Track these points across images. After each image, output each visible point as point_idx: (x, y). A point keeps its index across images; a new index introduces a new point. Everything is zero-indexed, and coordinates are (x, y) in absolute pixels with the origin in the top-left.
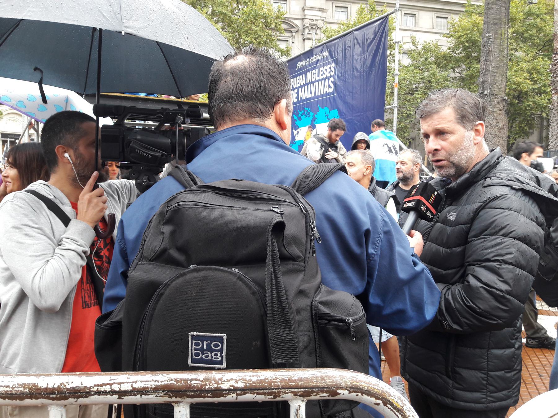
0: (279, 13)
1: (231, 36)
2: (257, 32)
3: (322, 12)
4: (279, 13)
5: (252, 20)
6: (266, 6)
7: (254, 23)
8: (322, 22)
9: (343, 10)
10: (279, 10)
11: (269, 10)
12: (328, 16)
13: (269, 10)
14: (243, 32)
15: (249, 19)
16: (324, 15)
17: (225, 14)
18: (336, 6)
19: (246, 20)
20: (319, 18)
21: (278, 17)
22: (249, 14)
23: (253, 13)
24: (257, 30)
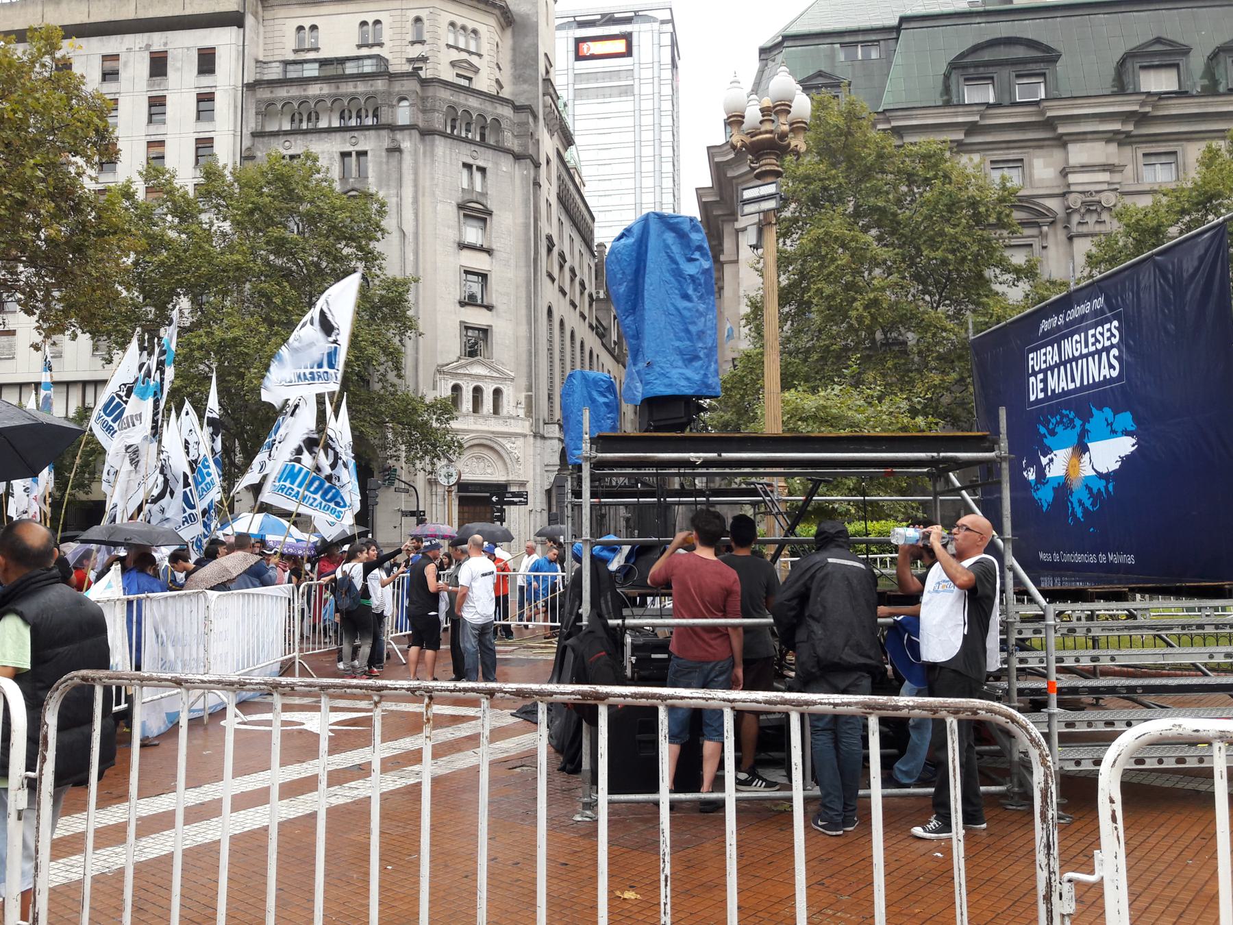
3: (1111, 171)
8: (1112, 195)
9: (1164, 159)
12: (1126, 179)
16: (1117, 178)
18: (1145, 155)
20: (1105, 187)
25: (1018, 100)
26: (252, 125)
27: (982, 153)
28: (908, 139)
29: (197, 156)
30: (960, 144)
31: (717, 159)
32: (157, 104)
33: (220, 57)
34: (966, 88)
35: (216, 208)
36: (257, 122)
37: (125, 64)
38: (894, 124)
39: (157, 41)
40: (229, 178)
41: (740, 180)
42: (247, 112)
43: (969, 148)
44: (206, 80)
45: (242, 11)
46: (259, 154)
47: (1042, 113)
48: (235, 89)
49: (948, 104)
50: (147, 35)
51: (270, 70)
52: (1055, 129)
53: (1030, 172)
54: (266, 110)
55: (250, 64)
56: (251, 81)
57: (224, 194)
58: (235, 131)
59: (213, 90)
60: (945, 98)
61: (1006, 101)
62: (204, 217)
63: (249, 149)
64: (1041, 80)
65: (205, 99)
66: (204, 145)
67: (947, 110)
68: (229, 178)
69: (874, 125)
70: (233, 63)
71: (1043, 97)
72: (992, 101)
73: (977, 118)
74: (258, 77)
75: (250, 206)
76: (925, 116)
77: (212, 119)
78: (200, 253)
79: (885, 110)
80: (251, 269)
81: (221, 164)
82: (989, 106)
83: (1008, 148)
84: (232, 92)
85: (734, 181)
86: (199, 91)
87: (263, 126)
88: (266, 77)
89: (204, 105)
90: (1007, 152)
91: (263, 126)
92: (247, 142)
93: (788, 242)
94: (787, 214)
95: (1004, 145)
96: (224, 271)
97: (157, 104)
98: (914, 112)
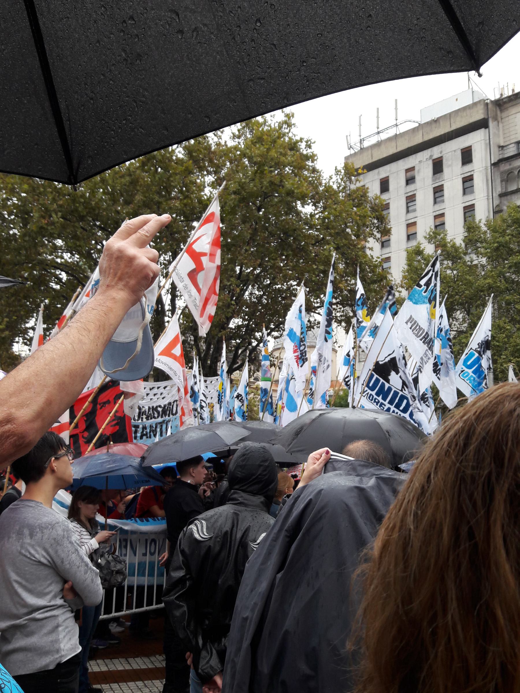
26: (499, 190)
29: (465, 218)
32: (438, 191)
33: (475, 151)
35: (476, 249)
36: (502, 187)
37: (419, 172)
39: (436, 152)
40: (484, 228)
42: (495, 182)
44: (468, 168)
45: (486, 117)
46: (505, 208)
48: (486, 169)
50: (430, 150)
51: (508, 151)
54: (507, 177)
55: (495, 149)
56: (496, 161)
57: (480, 240)
58: (488, 196)
59: (472, 173)
62: (467, 258)
63: (498, 206)
65: (468, 180)
66: (469, 210)
68: (484, 228)
70: (484, 152)
74: (501, 157)
75: (496, 245)
77: (472, 192)
78: (464, 282)
80: (499, 287)
81: (477, 221)
84: (484, 172)
86: (463, 176)
87: (506, 188)
88: (506, 156)
89: (467, 184)
91: (506, 188)
92: (497, 202)
96: (482, 291)
97: (438, 191)
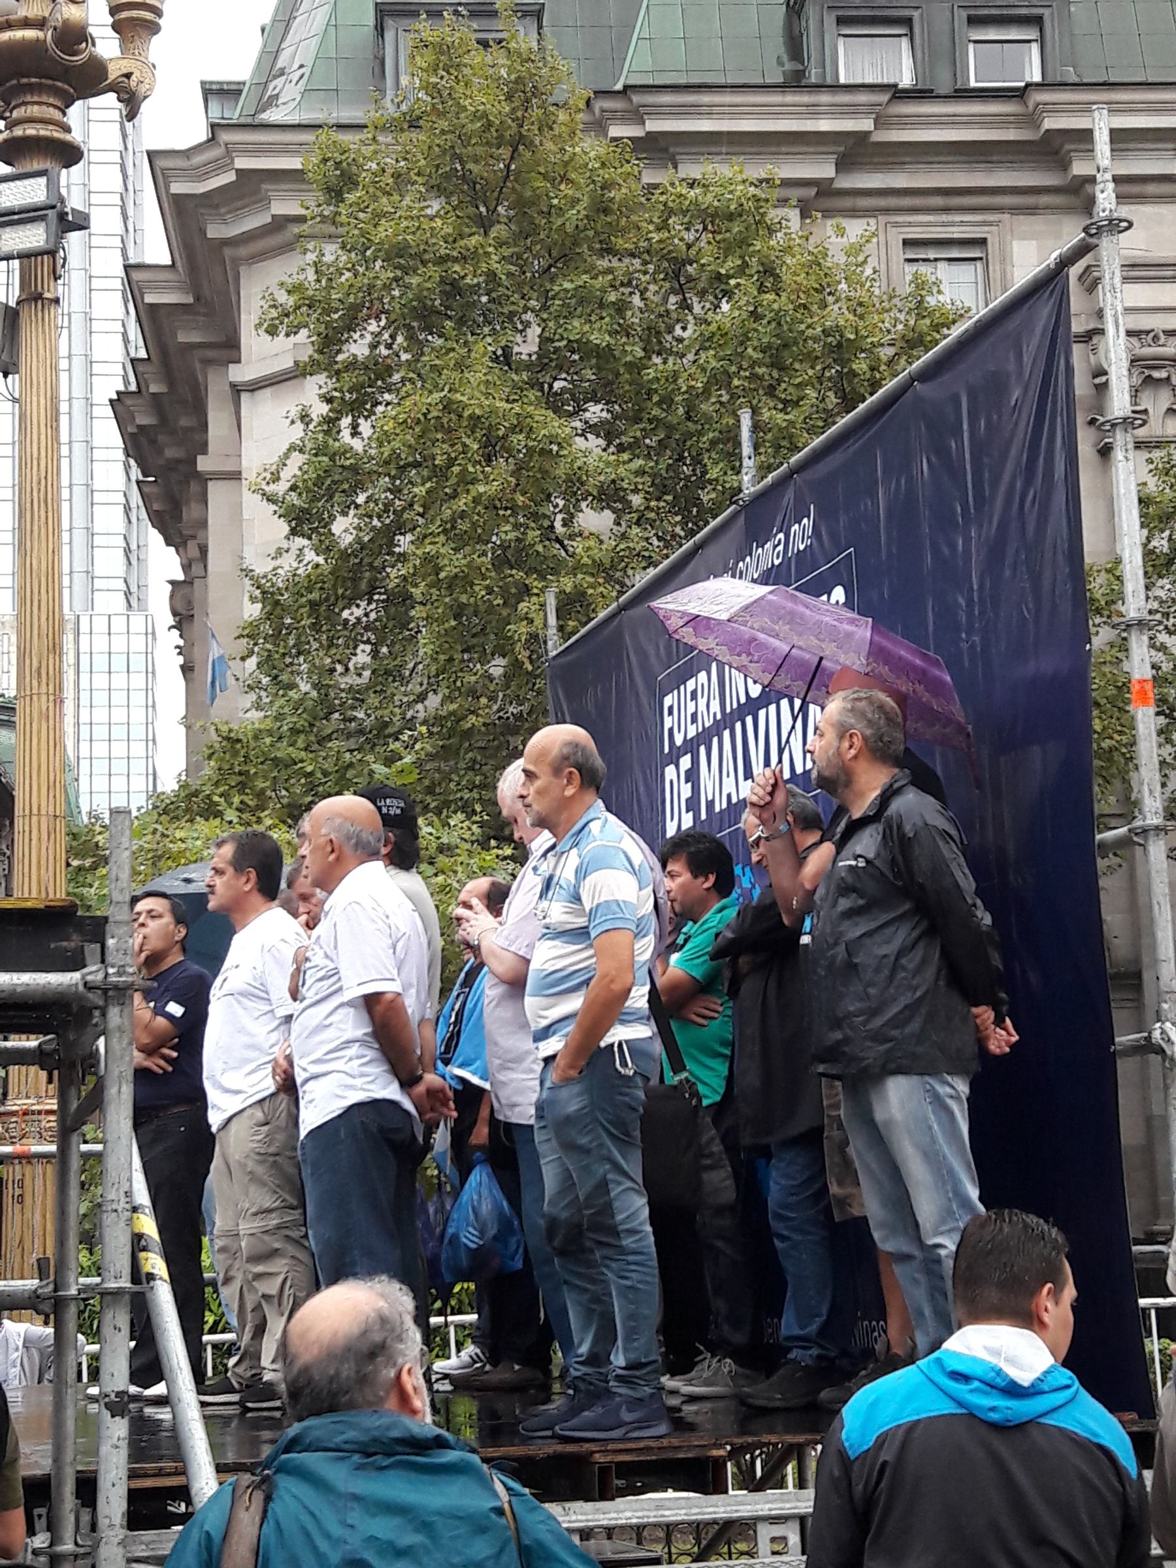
0: (920, 317)
1: (641, 472)
2: (791, 436)
4: (920, 317)
5: (761, 371)
6: (843, 286)
7: (771, 391)
10: (920, 302)
11: (859, 308)
13: (861, 304)
14: (713, 443)
15: (741, 368)
17: (603, 356)
19: (726, 372)
21: (913, 343)
22: (744, 340)
23: (764, 333)
24: (791, 422)
25: (973, 84)
27: (882, 219)
28: (691, 170)
30: (824, 189)
31: (177, 188)
34: (841, 41)
38: (653, 125)
41: (243, 251)
43: (848, 202)
47: (1031, 119)
49: (796, 82)
52: (1065, 166)
53: (1004, 272)
60: (789, 66)
61: (944, 88)
64: (1032, 34)
67: (789, 98)
69: (599, 127)
71: (1037, 78)
72: (906, 80)
73: (866, 124)
76: (735, 112)
79: (626, 88)
82: (898, 94)
83: (946, 210)
85: (228, 252)
90: (944, 218)
93: (365, 427)
94: (358, 348)
95: (938, 201)
98: (706, 98)
